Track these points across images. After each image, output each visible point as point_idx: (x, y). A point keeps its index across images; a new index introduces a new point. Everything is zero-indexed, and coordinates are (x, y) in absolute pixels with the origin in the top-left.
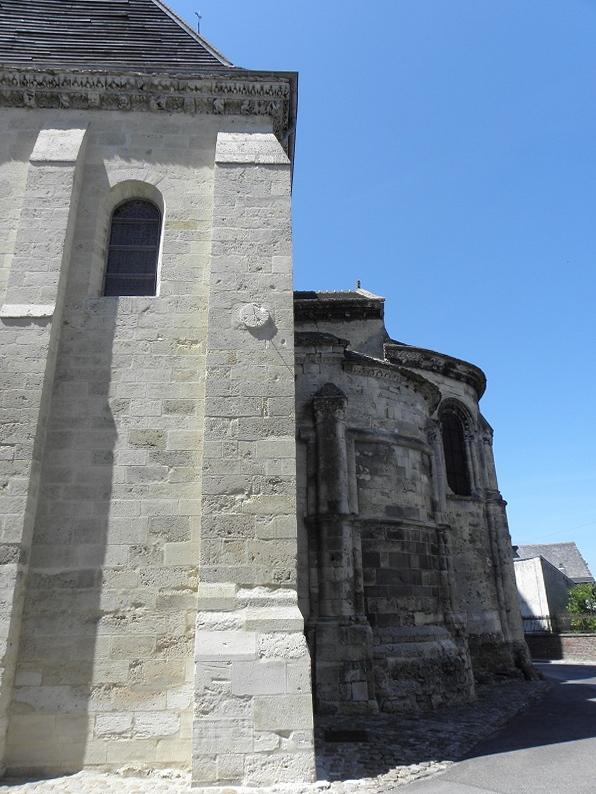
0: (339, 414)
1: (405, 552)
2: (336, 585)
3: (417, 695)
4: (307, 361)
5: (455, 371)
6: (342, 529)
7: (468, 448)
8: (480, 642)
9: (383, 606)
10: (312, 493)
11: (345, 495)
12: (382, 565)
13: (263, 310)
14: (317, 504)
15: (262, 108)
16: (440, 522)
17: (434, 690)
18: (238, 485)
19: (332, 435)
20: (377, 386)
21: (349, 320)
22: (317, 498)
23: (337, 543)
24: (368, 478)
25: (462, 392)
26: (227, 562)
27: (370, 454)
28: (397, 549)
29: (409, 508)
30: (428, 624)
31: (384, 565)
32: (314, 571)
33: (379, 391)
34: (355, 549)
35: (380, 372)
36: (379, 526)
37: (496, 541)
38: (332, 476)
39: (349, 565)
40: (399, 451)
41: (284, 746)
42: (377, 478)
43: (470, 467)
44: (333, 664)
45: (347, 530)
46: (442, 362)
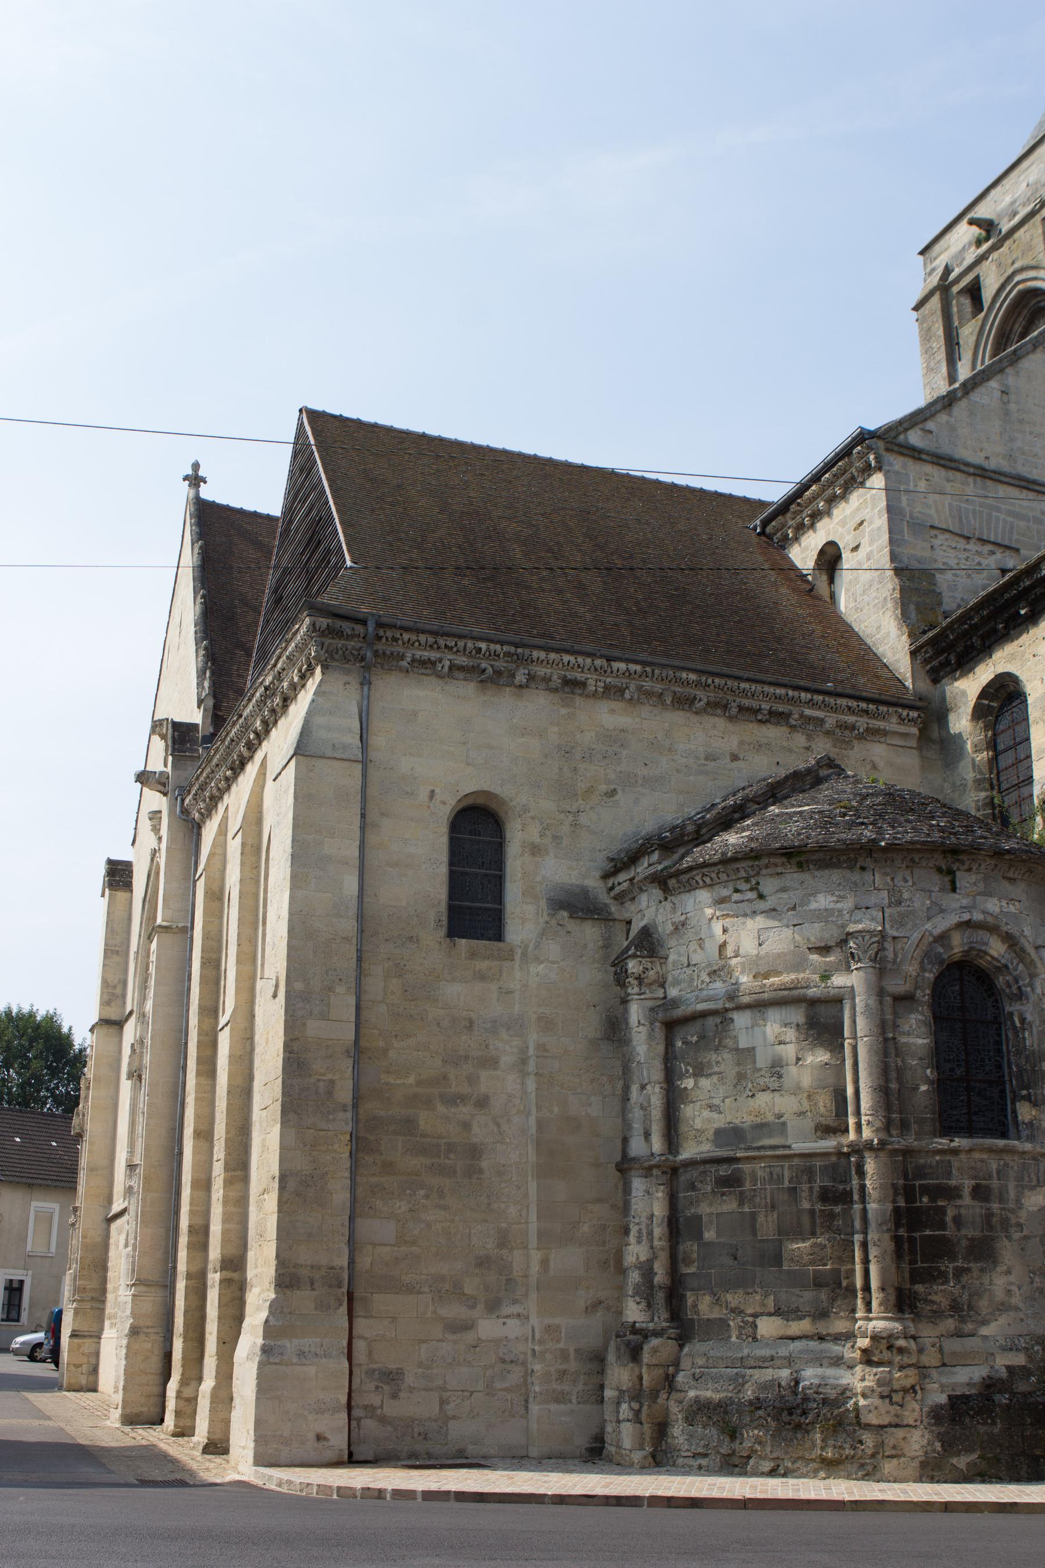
6: (631, 1182)
20: (710, 900)
27: (695, 1038)
28: (729, 1205)
30: (793, 1339)
31: (709, 1235)
35: (704, 875)
36: (702, 1168)
39: (639, 1242)
40: (741, 1020)
42: (705, 1083)
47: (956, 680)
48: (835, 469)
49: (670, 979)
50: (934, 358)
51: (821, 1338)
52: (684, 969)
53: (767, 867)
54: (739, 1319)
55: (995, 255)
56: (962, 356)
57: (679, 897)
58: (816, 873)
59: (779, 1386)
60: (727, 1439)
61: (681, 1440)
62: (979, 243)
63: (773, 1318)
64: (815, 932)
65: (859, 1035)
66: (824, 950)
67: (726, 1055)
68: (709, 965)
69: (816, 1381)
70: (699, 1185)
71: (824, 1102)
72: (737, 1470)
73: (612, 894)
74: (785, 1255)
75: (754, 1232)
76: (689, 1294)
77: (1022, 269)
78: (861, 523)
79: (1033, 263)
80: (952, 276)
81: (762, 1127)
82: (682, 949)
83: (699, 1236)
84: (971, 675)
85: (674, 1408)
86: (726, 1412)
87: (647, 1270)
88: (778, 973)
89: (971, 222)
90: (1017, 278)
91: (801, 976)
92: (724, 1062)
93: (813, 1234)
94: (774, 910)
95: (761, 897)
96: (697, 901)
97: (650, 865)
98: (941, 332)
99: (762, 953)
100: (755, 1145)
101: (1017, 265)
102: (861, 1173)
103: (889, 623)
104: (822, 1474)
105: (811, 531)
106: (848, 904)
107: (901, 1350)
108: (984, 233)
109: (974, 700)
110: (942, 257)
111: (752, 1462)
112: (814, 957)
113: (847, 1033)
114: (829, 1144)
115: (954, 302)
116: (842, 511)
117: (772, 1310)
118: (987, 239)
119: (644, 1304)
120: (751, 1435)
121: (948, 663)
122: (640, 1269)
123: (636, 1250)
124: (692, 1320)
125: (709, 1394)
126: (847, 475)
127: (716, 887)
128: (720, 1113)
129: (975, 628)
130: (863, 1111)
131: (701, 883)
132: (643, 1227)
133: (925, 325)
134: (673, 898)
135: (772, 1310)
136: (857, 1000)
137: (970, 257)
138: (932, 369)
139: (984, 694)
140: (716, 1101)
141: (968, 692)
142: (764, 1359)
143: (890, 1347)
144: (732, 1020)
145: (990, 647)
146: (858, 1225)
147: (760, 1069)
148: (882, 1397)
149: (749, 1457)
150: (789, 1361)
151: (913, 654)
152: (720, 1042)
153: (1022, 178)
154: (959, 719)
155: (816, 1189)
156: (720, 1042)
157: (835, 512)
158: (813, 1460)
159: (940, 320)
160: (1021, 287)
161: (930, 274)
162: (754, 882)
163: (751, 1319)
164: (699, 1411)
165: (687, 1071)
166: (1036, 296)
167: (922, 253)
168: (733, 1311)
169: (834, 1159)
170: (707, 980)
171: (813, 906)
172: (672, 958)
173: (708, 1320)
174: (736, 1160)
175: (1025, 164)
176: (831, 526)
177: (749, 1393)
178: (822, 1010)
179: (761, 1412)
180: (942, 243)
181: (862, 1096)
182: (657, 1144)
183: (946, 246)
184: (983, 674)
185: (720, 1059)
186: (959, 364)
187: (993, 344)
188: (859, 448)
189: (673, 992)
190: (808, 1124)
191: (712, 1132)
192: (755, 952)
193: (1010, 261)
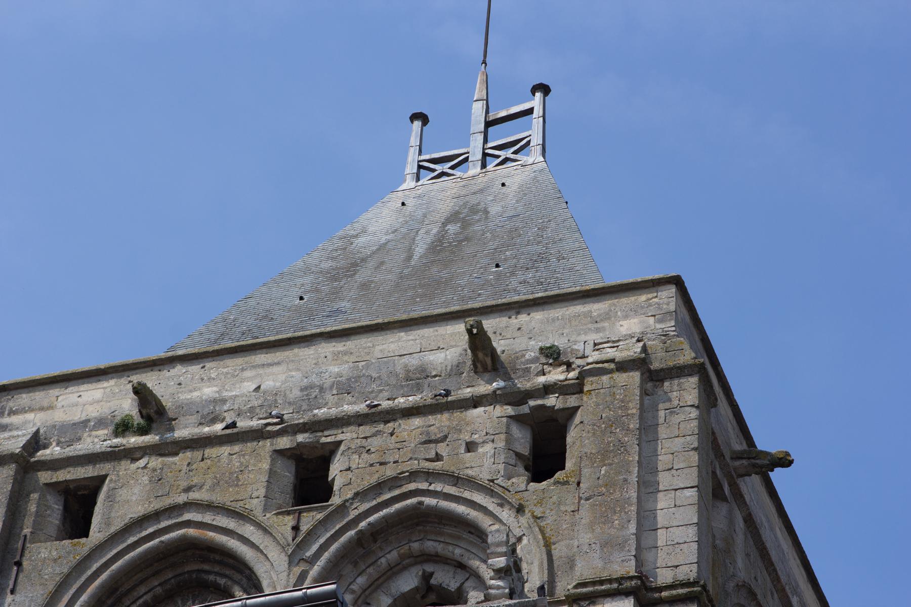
55: (155, 462)
56: (18, 588)
62: (123, 427)
77: (209, 507)
79: (237, 506)
80: (43, 454)
89: (141, 392)
90: (187, 516)
101: (194, 495)
108: (137, 420)
110: (30, 416)
115: (35, 496)
118: (143, 431)
153: (248, 374)
160: (192, 532)
166: (205, 560)
175: (261, 358)
180: (39, 396)
183: (45, 404)
186: (9, 598)
187: (92, 596)
193: (184, 484)
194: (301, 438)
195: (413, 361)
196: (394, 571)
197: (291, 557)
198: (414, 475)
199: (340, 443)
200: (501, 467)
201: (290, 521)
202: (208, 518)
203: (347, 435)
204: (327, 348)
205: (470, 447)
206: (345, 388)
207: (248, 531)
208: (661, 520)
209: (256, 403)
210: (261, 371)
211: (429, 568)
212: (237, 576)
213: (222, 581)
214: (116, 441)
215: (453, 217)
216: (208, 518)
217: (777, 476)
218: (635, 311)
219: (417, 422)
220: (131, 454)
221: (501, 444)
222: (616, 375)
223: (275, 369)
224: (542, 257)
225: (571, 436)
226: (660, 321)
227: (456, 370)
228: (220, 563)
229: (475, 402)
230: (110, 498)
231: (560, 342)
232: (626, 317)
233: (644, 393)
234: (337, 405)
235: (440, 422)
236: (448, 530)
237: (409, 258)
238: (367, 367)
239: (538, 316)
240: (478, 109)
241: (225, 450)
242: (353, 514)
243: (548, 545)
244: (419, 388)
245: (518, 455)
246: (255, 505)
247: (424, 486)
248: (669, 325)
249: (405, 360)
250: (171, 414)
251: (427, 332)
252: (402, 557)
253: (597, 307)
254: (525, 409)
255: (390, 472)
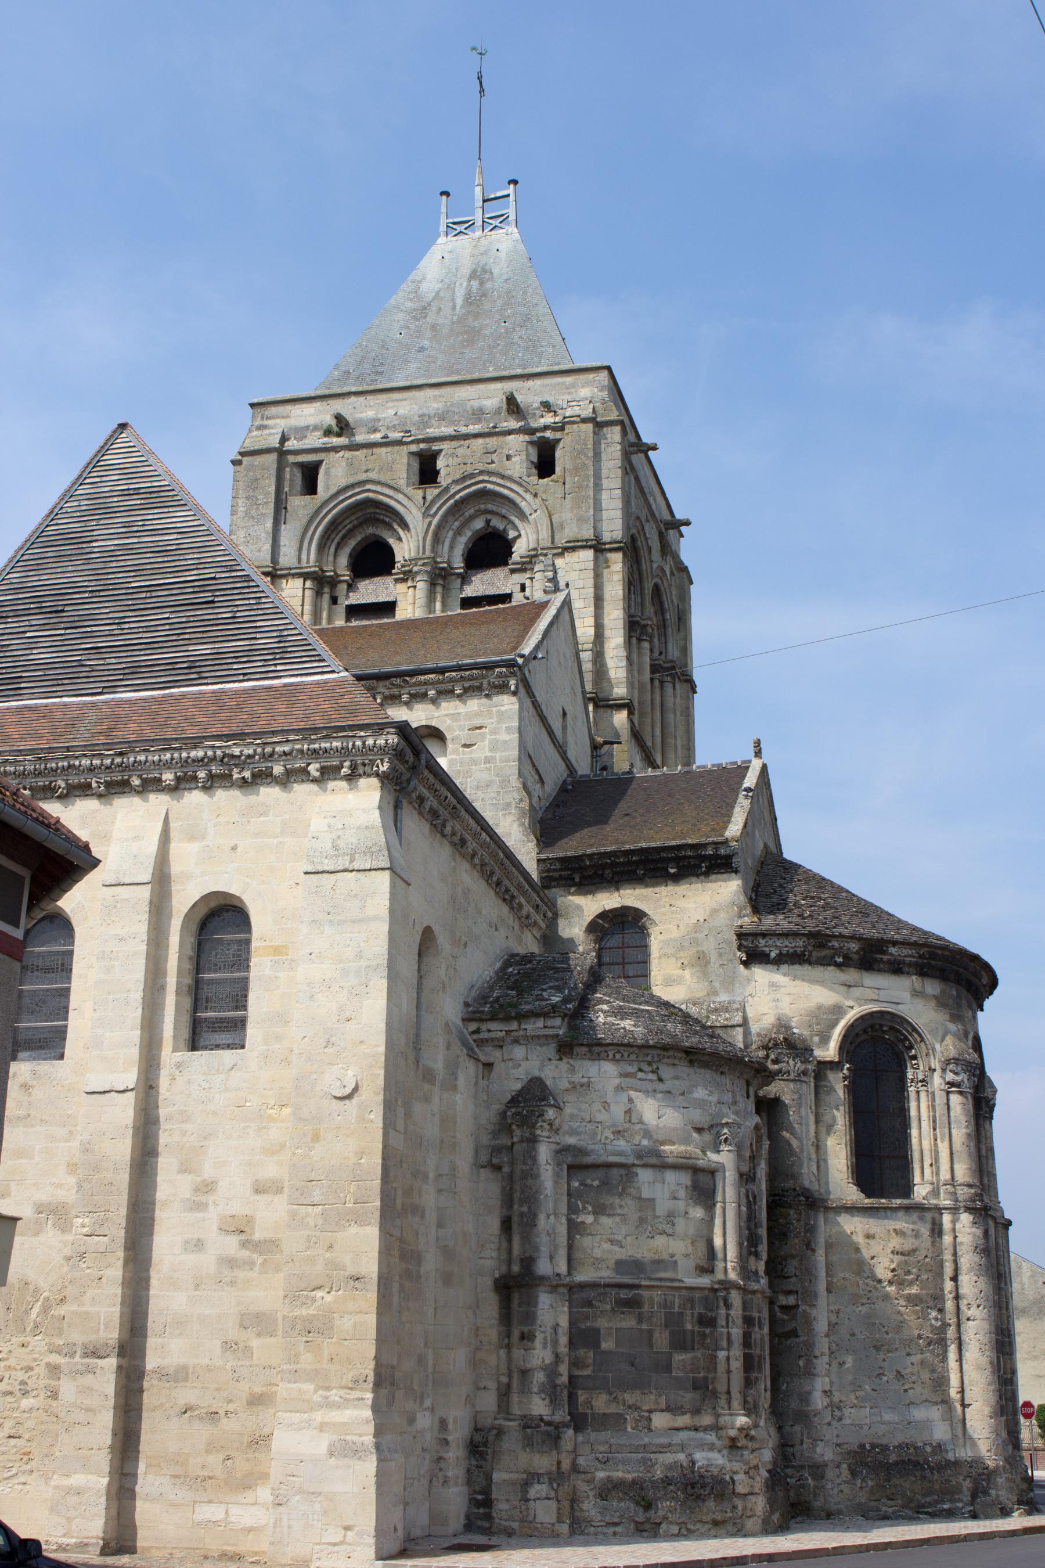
0: (542, 1132)
1: (644, 1327)
2: (525, 1373)
3: (636, 1523)
4: (508, 1040)
5: (885, 958)
6: (537, 1296)
7: (913, 1105)
8: (893, 1458)
9: (601, 1403)
10: (505, 1245)
11: (544, 1250)
12: (604, 1346)
13: (350, 1073)
14: (509, 1262)
15: (368, 769)
16: (720, 1275)
17: (665, 1518)
18: (319, 1283)
19: (529, 1162)
20: (616, 1073)
21: (676, 879)
22: (510, 1252)
23: (529, 1317)
24: (589, 1219)
25: (906, 996)
26: (307, 1360)
27: (596, 1183)
28: (628, 1322)
29: (658, 1262)
30: (678, 1429)
31: (607, 1345)
32: (503, 1353)
33: (617, 1081)
34: (556, 1327)
35: (619, 1052)
37: (955, 1279)
38: (530, 1222)
39: (545, 1348)
40: (644, 1176)
41: (349, 1539)
42: (605, 1220)
43: (914, 1141)
44: (514, 1476)
45: (544, 1300)
46: (854, 946)
47: (573, 894)
48: (467, 673)
49: (565, 1127)
50: (257, 509)
51: (696, 1429)
52: (584, 1124)
53: (669, 1057)
54: (636, 1414)
55: (348, 454)
57: (579, 1062)
58: (697, 1070)
59: (682, 1466)
60: (641, 1509)
61: (593, 1513)
63: (665, 1414)
64: (697, 1116)
65: (727, 1200)
66: (699, 1130)
67: (629, 1201)
68: (614, 1125)
69: (706, 1462)
70: (596, 1303)
71: (702, 1247)
72: (645, 1534)
73: (475, 1036)
74: (674, 1364)
75: (651, 1345)
76: (580, 1392)
78: (480, 728)
81: (658, 1263)
82: (584, 1106)
83: (596, 1345)
84: (590, 897)
85: (582, 1486)
86: (642, 1489)
87: (552, 1372)
88: (672, 1143)
90: (368, 487)
91: (689, 1148)
92: (629, 1207)
93: (693, 1349)
94: (669, 1092)
95: (660, 1080)
96: (602, 1070)
97: (545, 1027)
98: (272, 489)
99: (661, 1125)
100: (653, 1276)
102: (728, 1306)
103: (511, 826)
104: (713, 1532)
105: (405, 708)
106: (714, 1099)
107: (752, 1438)
108: (336, 429)
109: (592, 917)
110: (278, 421)
111: (664, 1526)
112: (695, 1135)
113: (719, 1198)
114: (705, 1281)
115: (288, 469)
116: (449, 707)
117: (664, 1407)
119: (548, 1400)
120: (664, 1506)
121: (570, 878)
122: (545, 1370)
123: (541, 1355)
124: (586, 1414)
125: (620, 1474)
126: (476, 683)
127: (622, 1063)
128: (622, 1247)
129: (614, 864)
130: (729, 1258)
131: (611, 1056)
132: (548, 1335)
133: (251, 474)
134: (571, 1061)
135: (664, 1407)
136: (727, 1174)
137: (315, 440)
138: (253, 518)
139: (603, 915)
140: (619, 1238)
141: (585, 908)
142: (663, 1446)
143: (746, 1436)
144: (637, 1175)
145: (617, 882)
146: (724, 1344)
147: (659, 1217)
148: (745, 1473)
149: (660, 1524)
150: (682, 1447)
151: (539, 861)
152: (624, 1190)
153: (390, 404)
154: (570, 925)
155: (696, 1315)
156: (624, 1190)
157: (444, 705)
158: (707, 1522)
159: (273, 479)
160: (371, 495)
161: (261, 428)
162: (655, 1067)
163: (646, 1414)
164: (608, 1490)
165: (584, 1208)
166: (377, 508)
167: (252, 405)
168: (630, 1407)
169: (706, 1292)
170: (612, 1137)
171: (696, 1095)
172: (568, 1110)
173: (604, 1414)
174: (638, 1287)
175: (396, 395)
176: (436, 714)
177: (658, 1472)
178: (703, 1178)
179: (671, 1488)
181: (728, 1247)
182: (563, 1269)
184: (608, 900)
185: (623, 1203)
186: (283, 527)
188: (504, 669)
189: (571, 1140)
190: (691, 1264)
191: (613, 1261)
192: (655, 1123)
193: (364, 468)
194: (422, 446)
195: (476, 404)
196: (472, 518)
197: (424, 514)
198: (481, 473)
199: (441, 450)
200: (525, 470)
201: (420, 493)
202: (379, 488)
203: (445, 446)
204: (430, 392)
205: (509, 457)
206: (442, 417)
207: (400, 497)
208: (604, 506)
209: (396, 423)
210: (396, 403)
211: (489, 517)
212: (394, 517)
213: (387, 520)
214: (326, 439)
215: (473, 275)
216: (379, 488)
217: (651, 453)
218: (588, 384)
219: (480, 441)
220: (335, 449)
221: (524, 457)
222: (581, 425)
223: (404, 403)
224: (527, 318)
225: (558, 453)
226: (600, 391)
227: (498, 411)
228: (386, 510)
229: (510, 432)
230: (327, 473)
231: (551, 399)
232: (583, 387)
233: (594, 433)
234: (439, 427)
235: (492, 442)
236: (498, 500)
237: (454, 307)
238: (452, 405)
239: (538, 383)
240: (478, 190)
241: (383, 450)
242: (452, 491)
243: (550, 516)
244: (479, 421)
245: (532, 462)
246: (402, 483)
247: (486, 478)
248: (605, 394)
249: (471, 403)
250: (352, 426)
251: (481, 387)
252: (476, 511)
253: (569, 379)
254: (535, 438)
255: (469, 469)
